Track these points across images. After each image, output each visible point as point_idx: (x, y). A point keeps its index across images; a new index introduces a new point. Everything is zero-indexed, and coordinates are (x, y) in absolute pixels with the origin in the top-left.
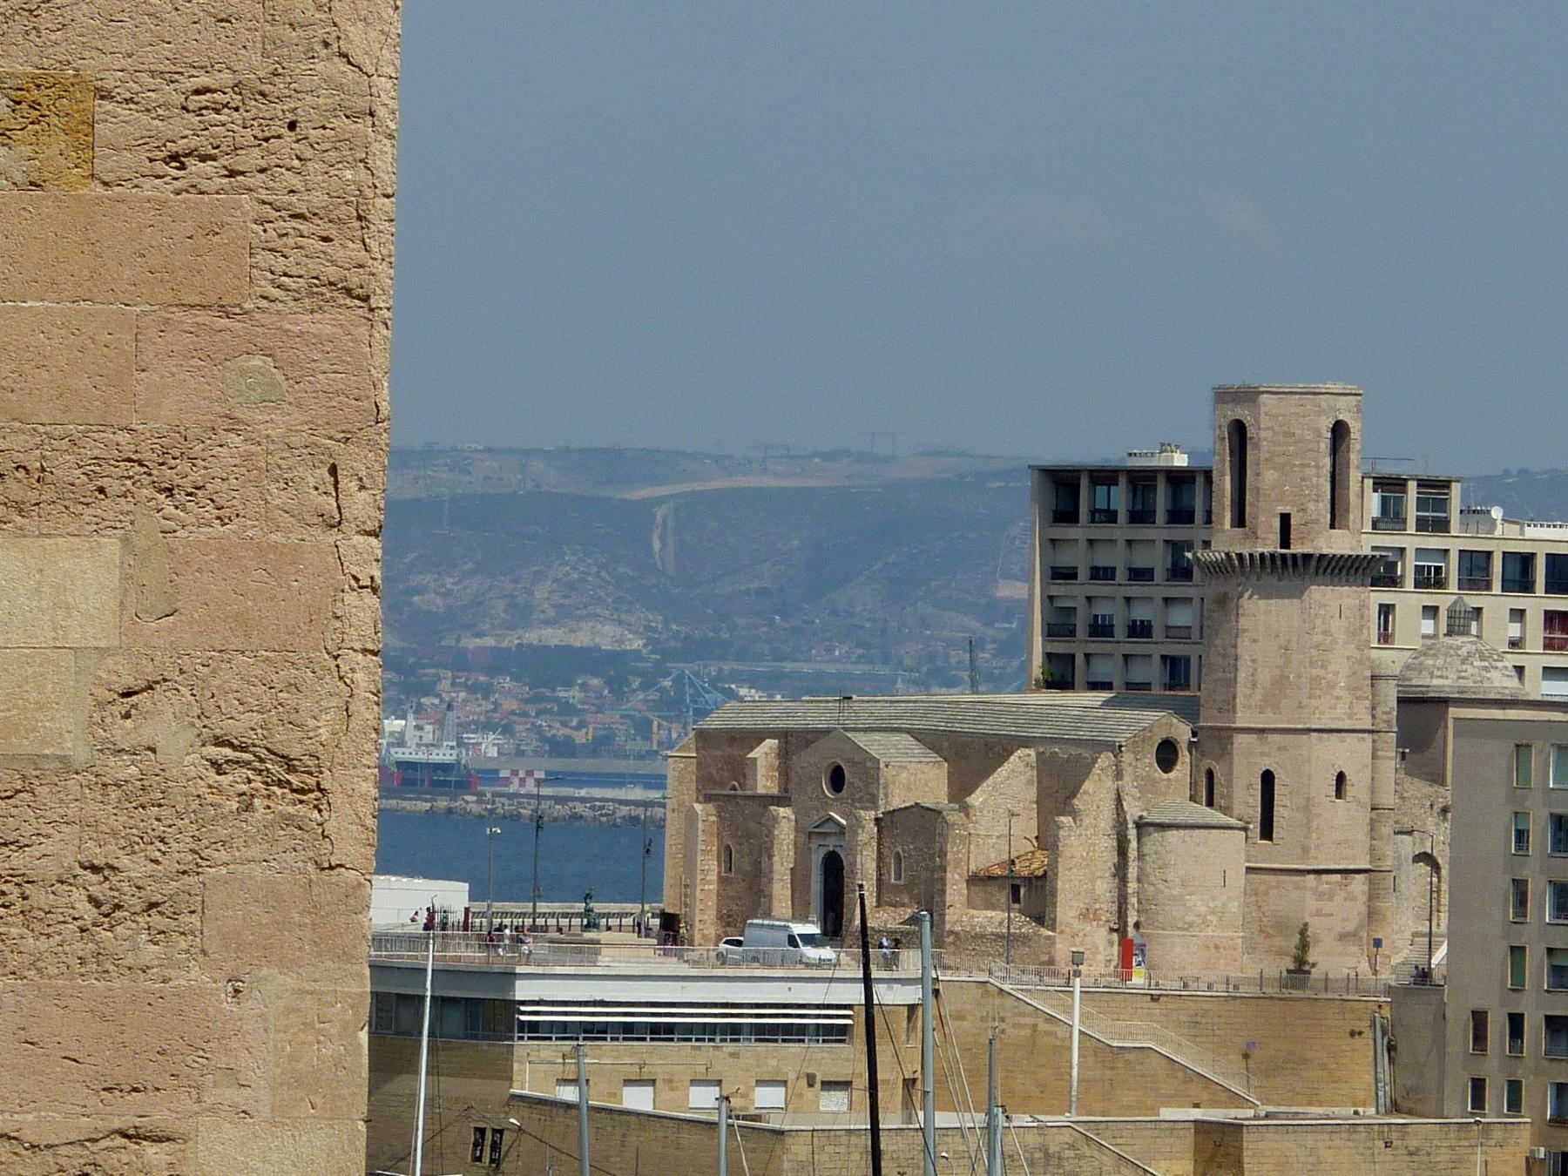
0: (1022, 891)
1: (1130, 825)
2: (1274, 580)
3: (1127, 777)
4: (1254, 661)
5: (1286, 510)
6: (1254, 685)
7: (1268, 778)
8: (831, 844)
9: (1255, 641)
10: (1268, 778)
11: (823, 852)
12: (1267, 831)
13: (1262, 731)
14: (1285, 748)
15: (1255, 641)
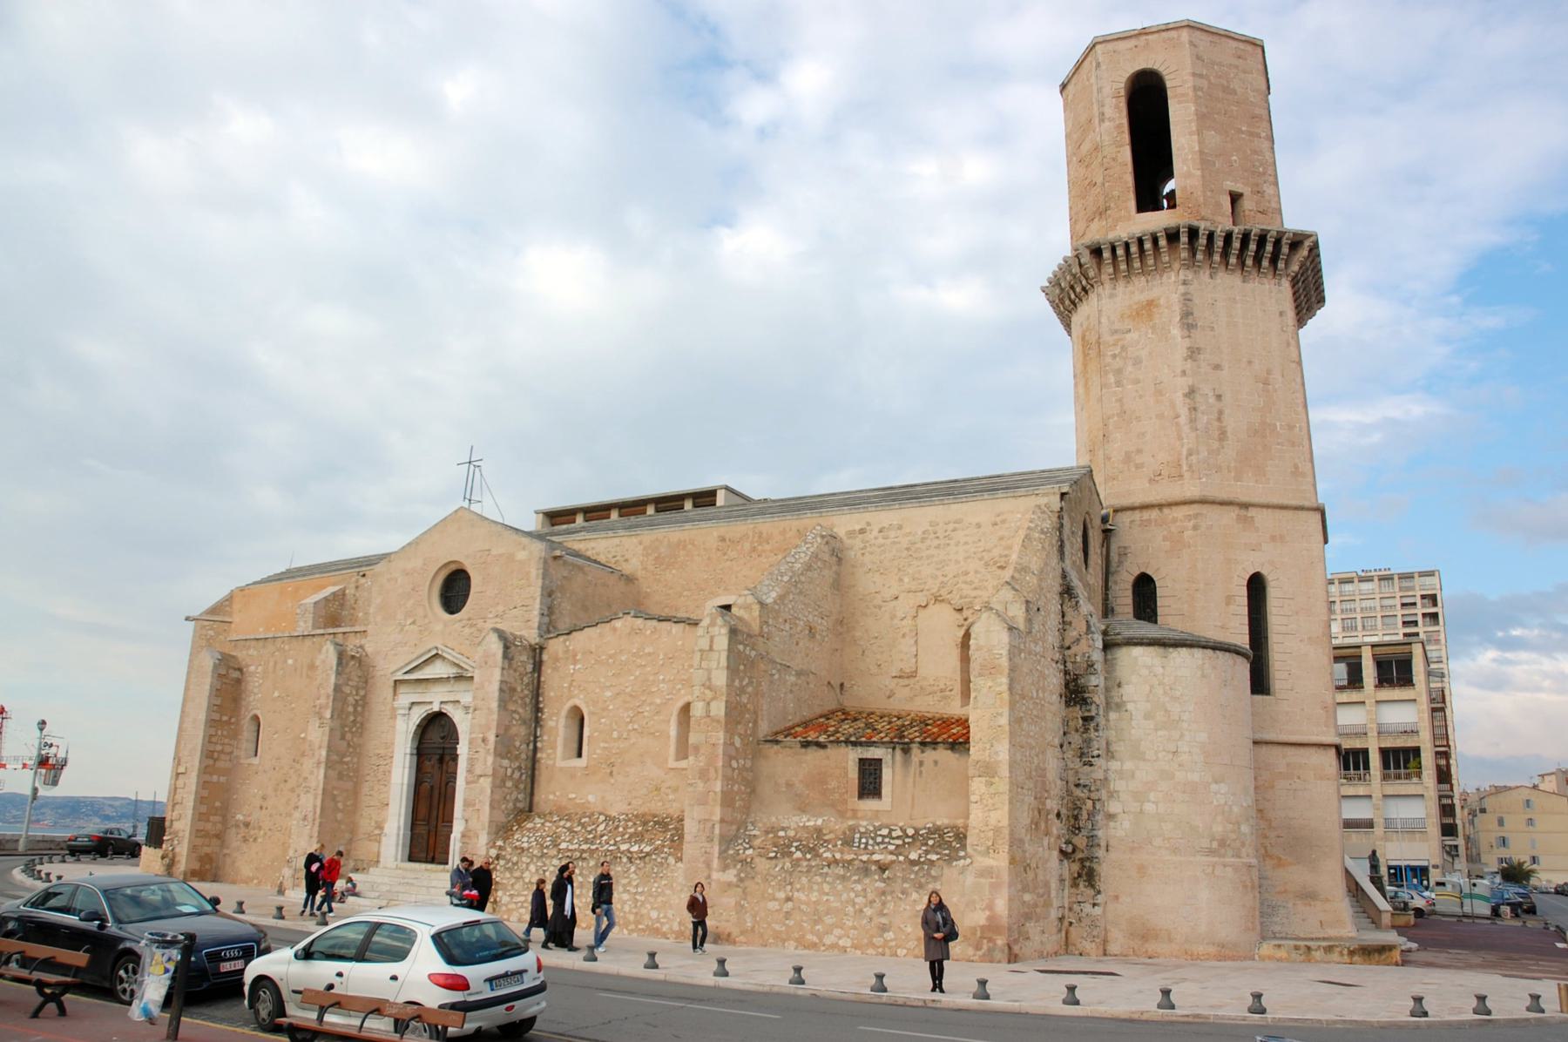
0: (886, 774)
1: (1099, 644)
2: (1235, 280)
3: (1068, 562)
4: (1219, 397)
5: (1238, 188)
6: (1223, 435)
7: (1256, 586)
8: (436, 699)
9: (1217, 367)
10: (1256, 586)
11: (418, 715)
12: (1260, 683)
13: (1245, 506)
14: (1282, 537)
15: (1217, 367)
